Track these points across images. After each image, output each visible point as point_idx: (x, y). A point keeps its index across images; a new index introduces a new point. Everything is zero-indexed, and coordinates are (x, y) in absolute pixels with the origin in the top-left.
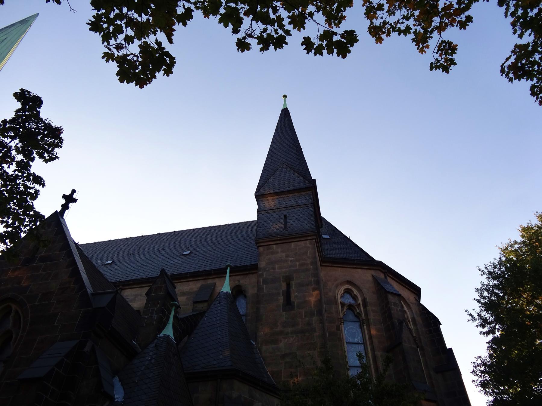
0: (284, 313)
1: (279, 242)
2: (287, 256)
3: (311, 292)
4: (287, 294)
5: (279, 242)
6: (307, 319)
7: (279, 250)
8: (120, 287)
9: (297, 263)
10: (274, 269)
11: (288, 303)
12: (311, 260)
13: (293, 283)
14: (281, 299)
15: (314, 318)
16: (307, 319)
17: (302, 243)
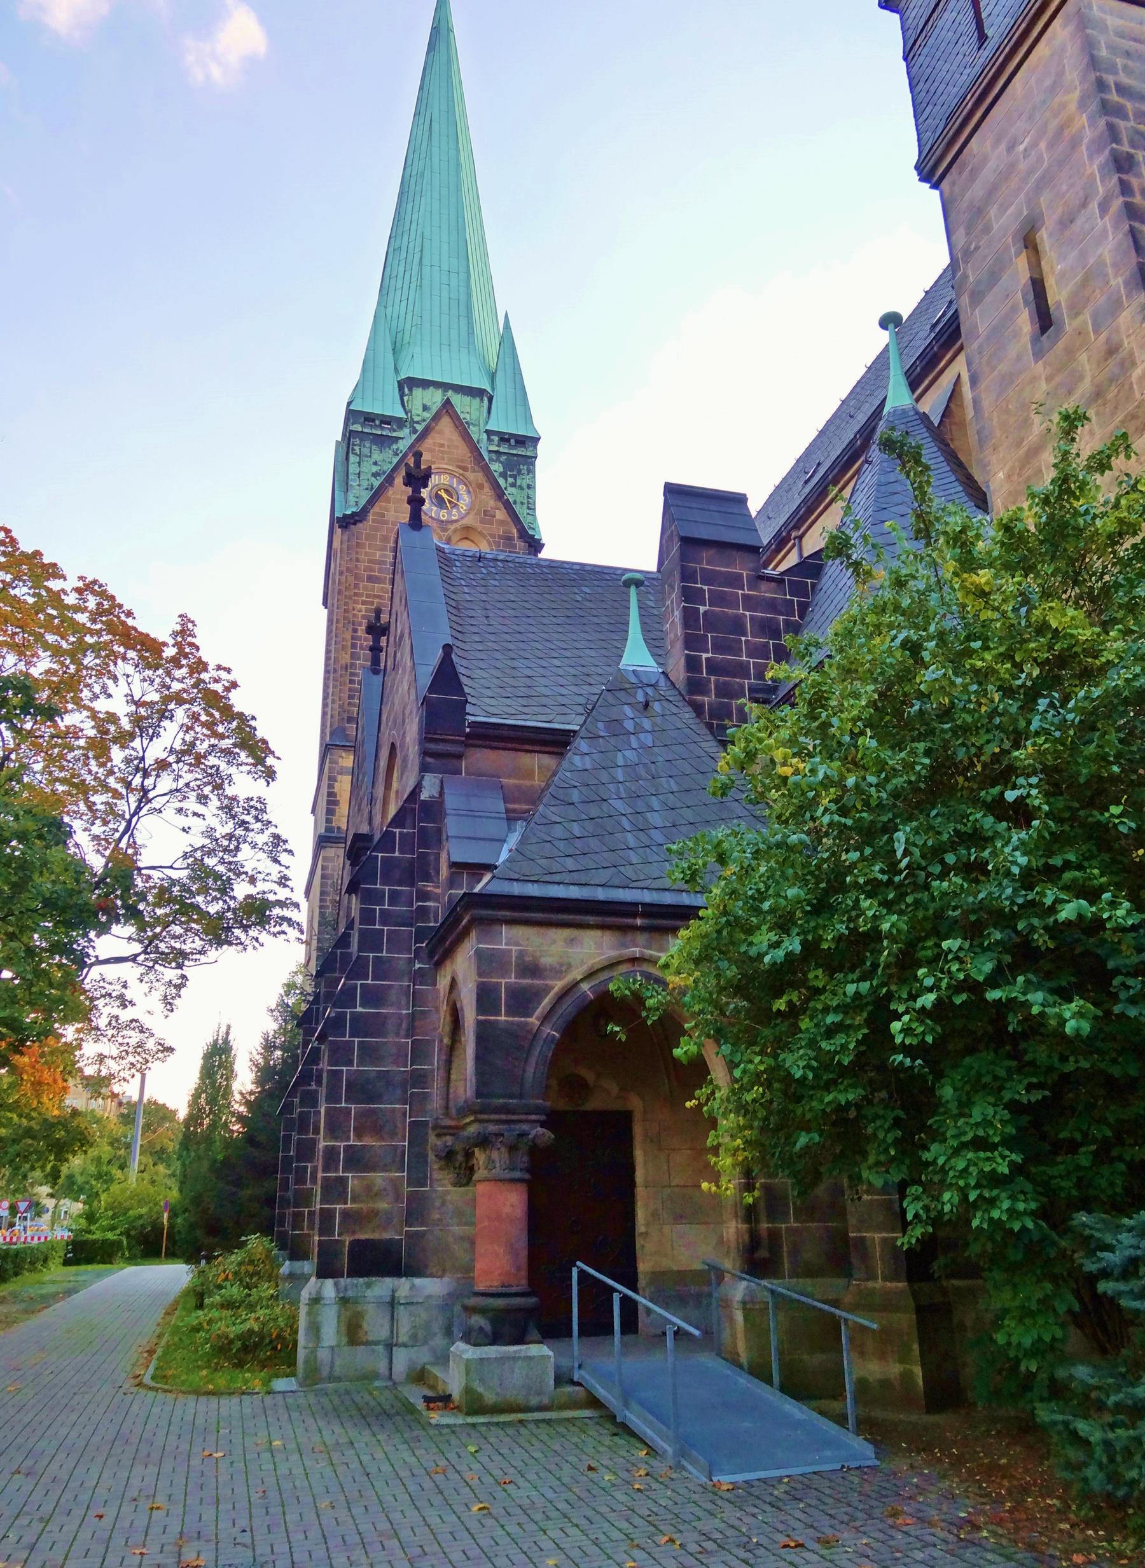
0: (1039, 368)
1: (978, 115)
2: (1011, 148)
3: (1100, 223)
4: (1038, 287)
5: (978, 115)
6: (1103, 337)
7: (988, 143)
8: (794, 534)
9: (1043, 145)
10: (987, 229)
11: (1045, 320)
12: (1076, 94)
13: (1044, 237)
14: (1025, 322)
15: (1125, 317)
16: (1103, 337)
17: (1042, 49)
